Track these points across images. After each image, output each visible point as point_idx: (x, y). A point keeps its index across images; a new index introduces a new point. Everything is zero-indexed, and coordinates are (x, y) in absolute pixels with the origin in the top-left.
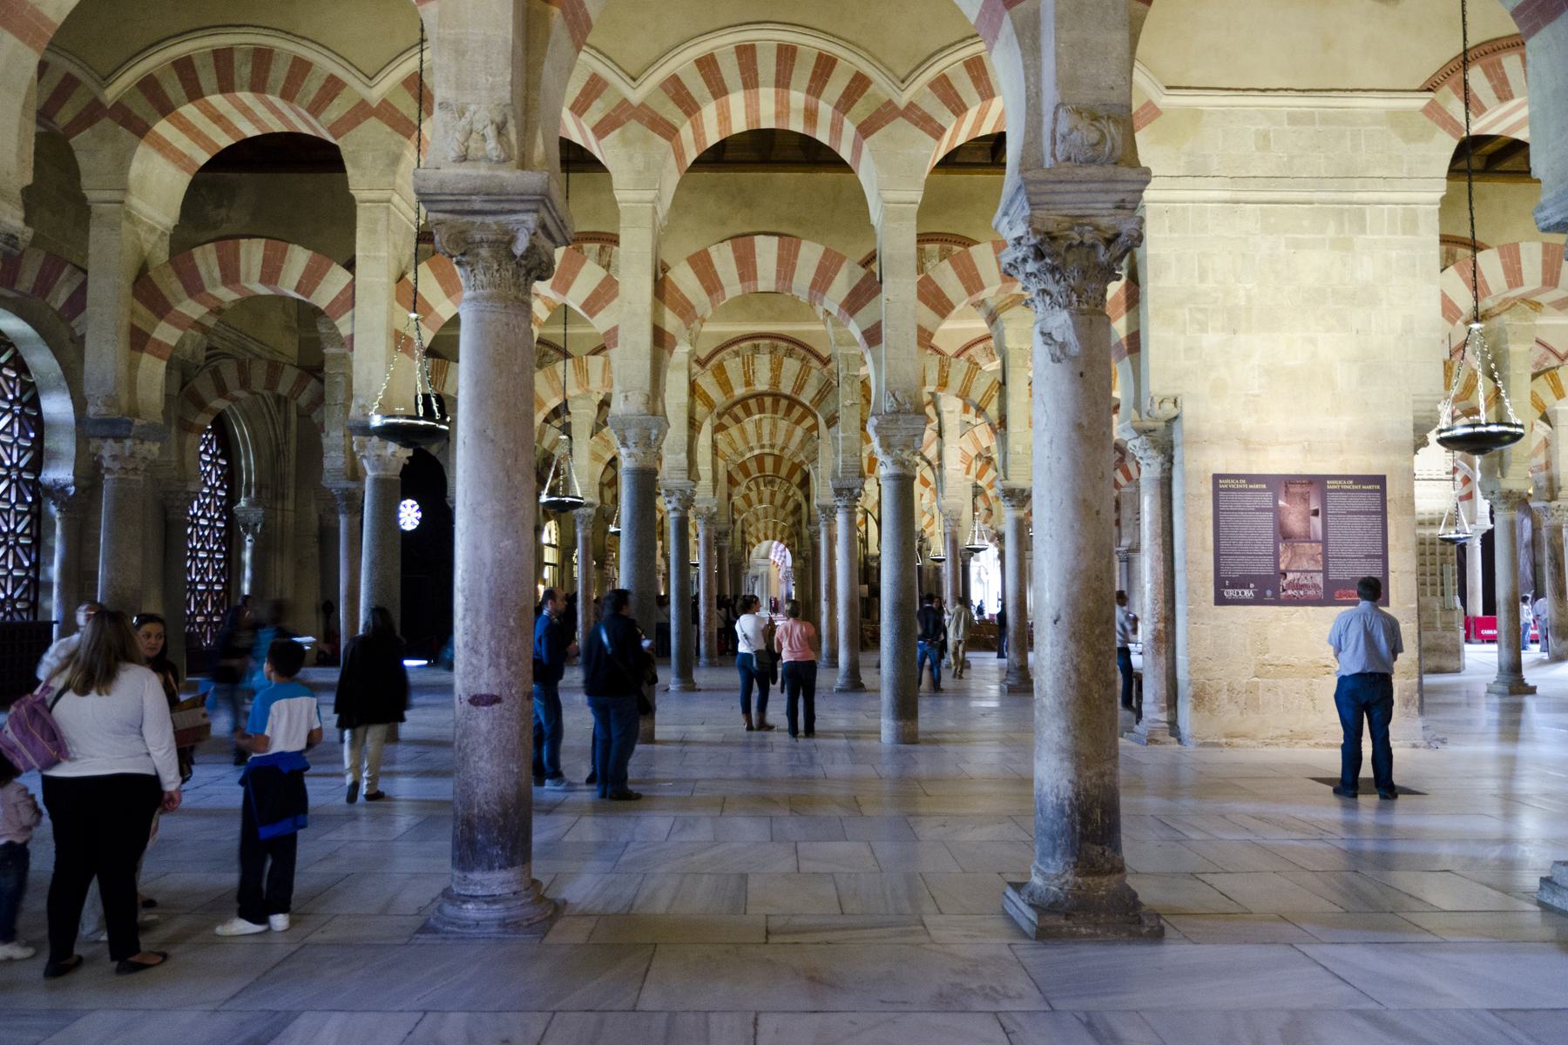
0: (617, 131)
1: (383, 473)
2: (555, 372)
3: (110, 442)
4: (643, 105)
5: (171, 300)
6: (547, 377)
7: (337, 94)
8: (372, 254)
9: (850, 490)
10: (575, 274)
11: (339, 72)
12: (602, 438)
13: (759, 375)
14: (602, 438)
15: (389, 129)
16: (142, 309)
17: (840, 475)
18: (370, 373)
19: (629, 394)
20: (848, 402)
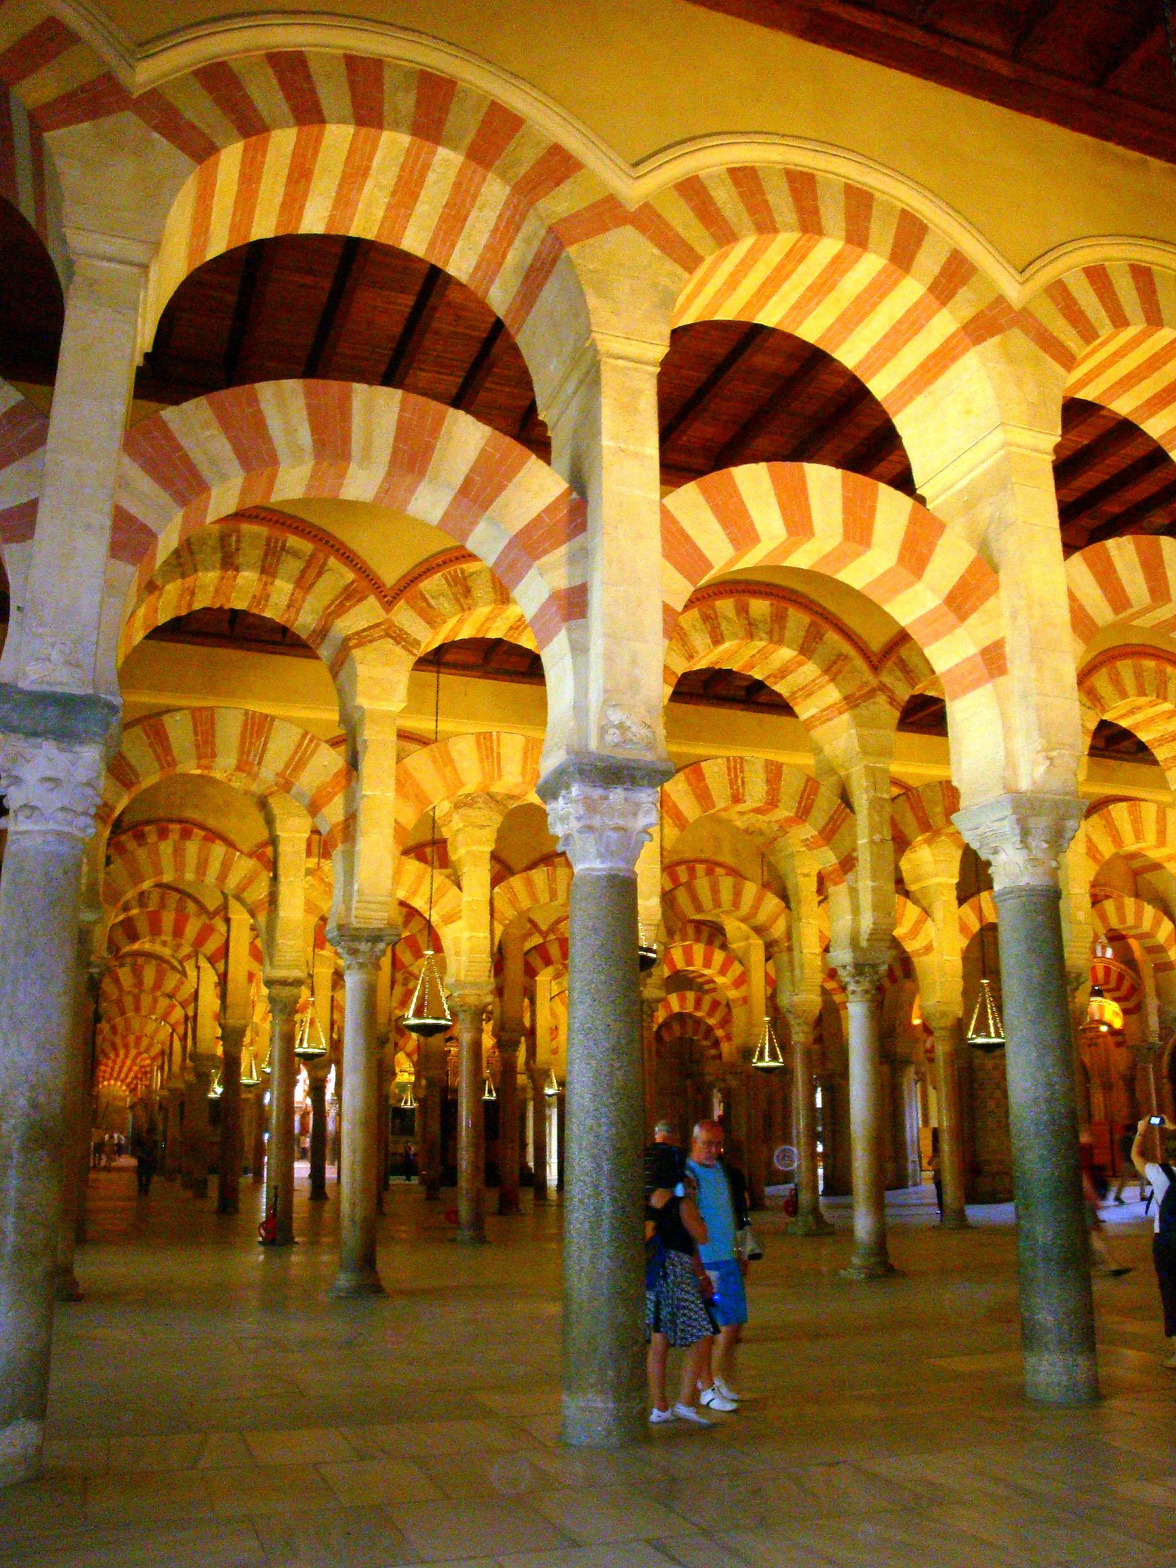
0: (997, 339)
1: (622, 865)
2: (448, 752)
3: (49, 748)
4: (1025, 309)
5: (205, 471)
6: (435, 761)
7: (567, 177)
8: (632, 447)
9: (874, 966)
10: (931, 547)
11: (573, 143)
12: (322, 880)
13: (749, 787)
14: (322, 880)
15: (656, 251)
16: (144, 482)
17: (864, 944)
18: (634, 662)
19: (1054, 754)
20: (877, 838)
